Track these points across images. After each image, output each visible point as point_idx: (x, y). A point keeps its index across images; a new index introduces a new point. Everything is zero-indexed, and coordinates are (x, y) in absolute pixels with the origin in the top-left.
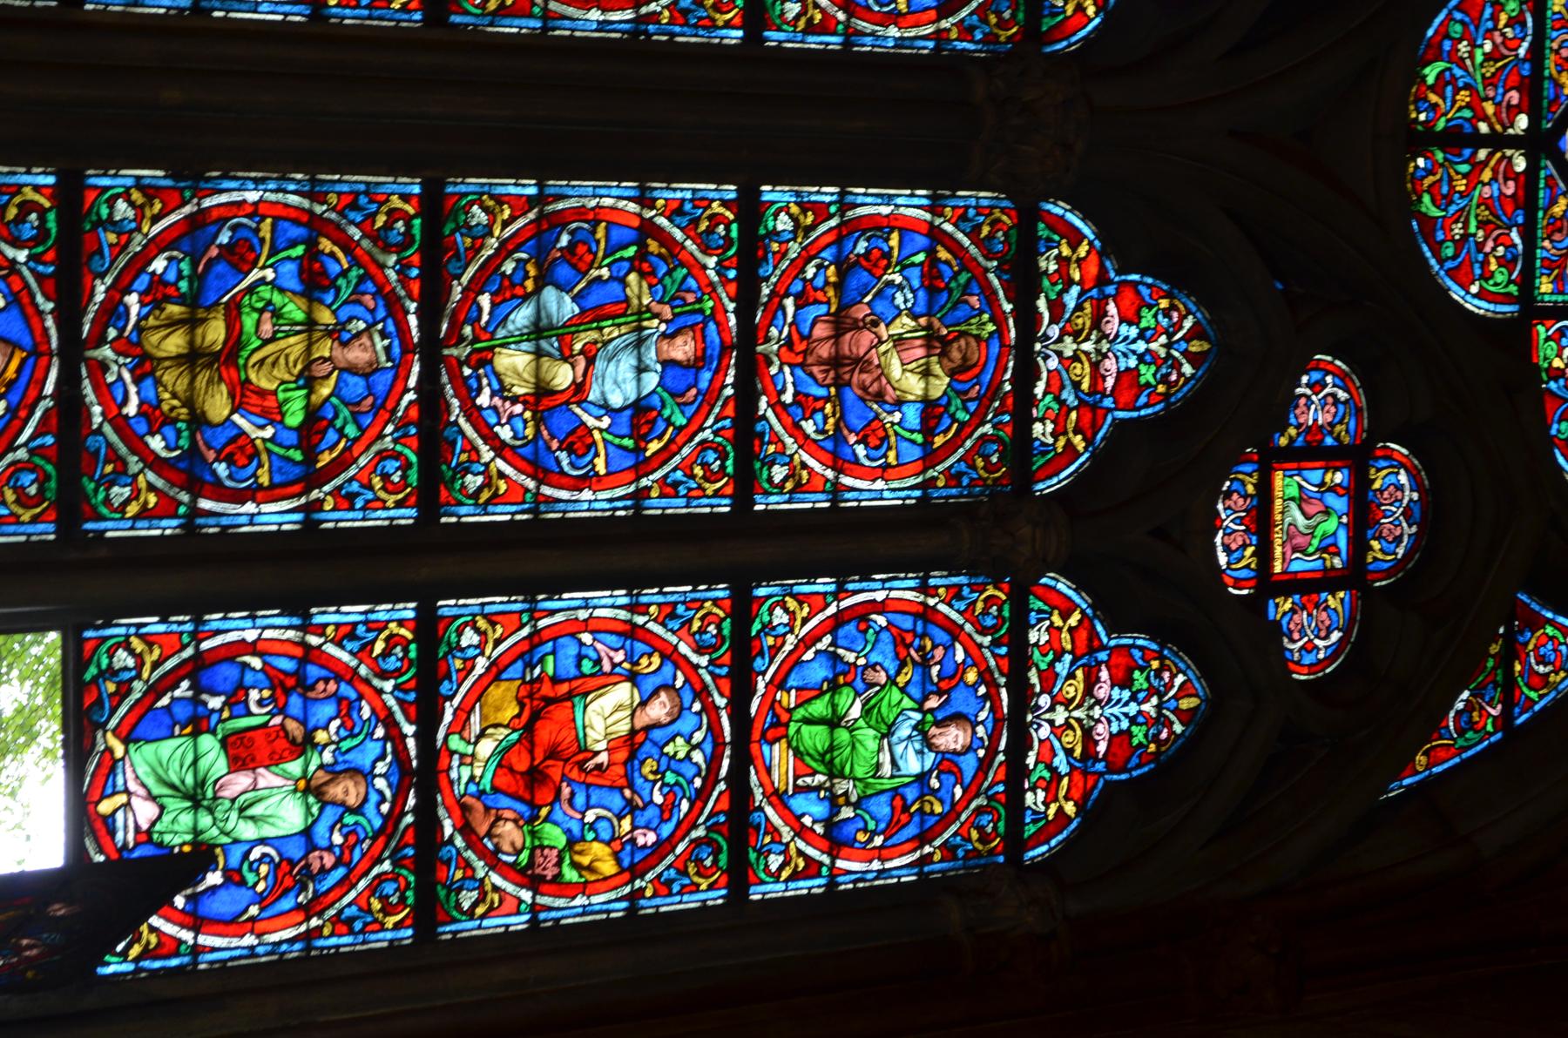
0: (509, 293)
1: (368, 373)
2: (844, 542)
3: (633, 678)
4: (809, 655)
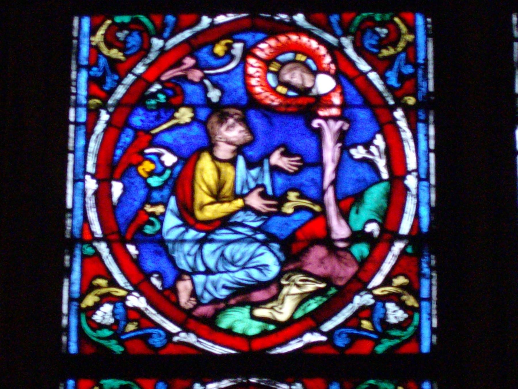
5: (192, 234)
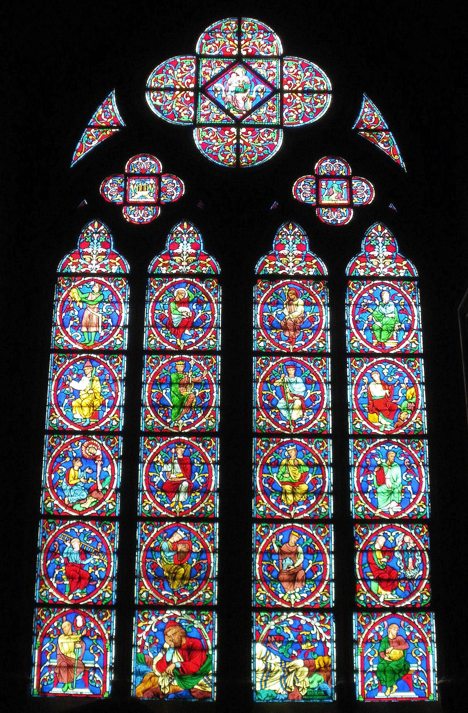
0: (279, 416)
1: (297, 450)
2: (338, 327)
3: (369, 384)
4: (365, 337)
5: (69, 487)
